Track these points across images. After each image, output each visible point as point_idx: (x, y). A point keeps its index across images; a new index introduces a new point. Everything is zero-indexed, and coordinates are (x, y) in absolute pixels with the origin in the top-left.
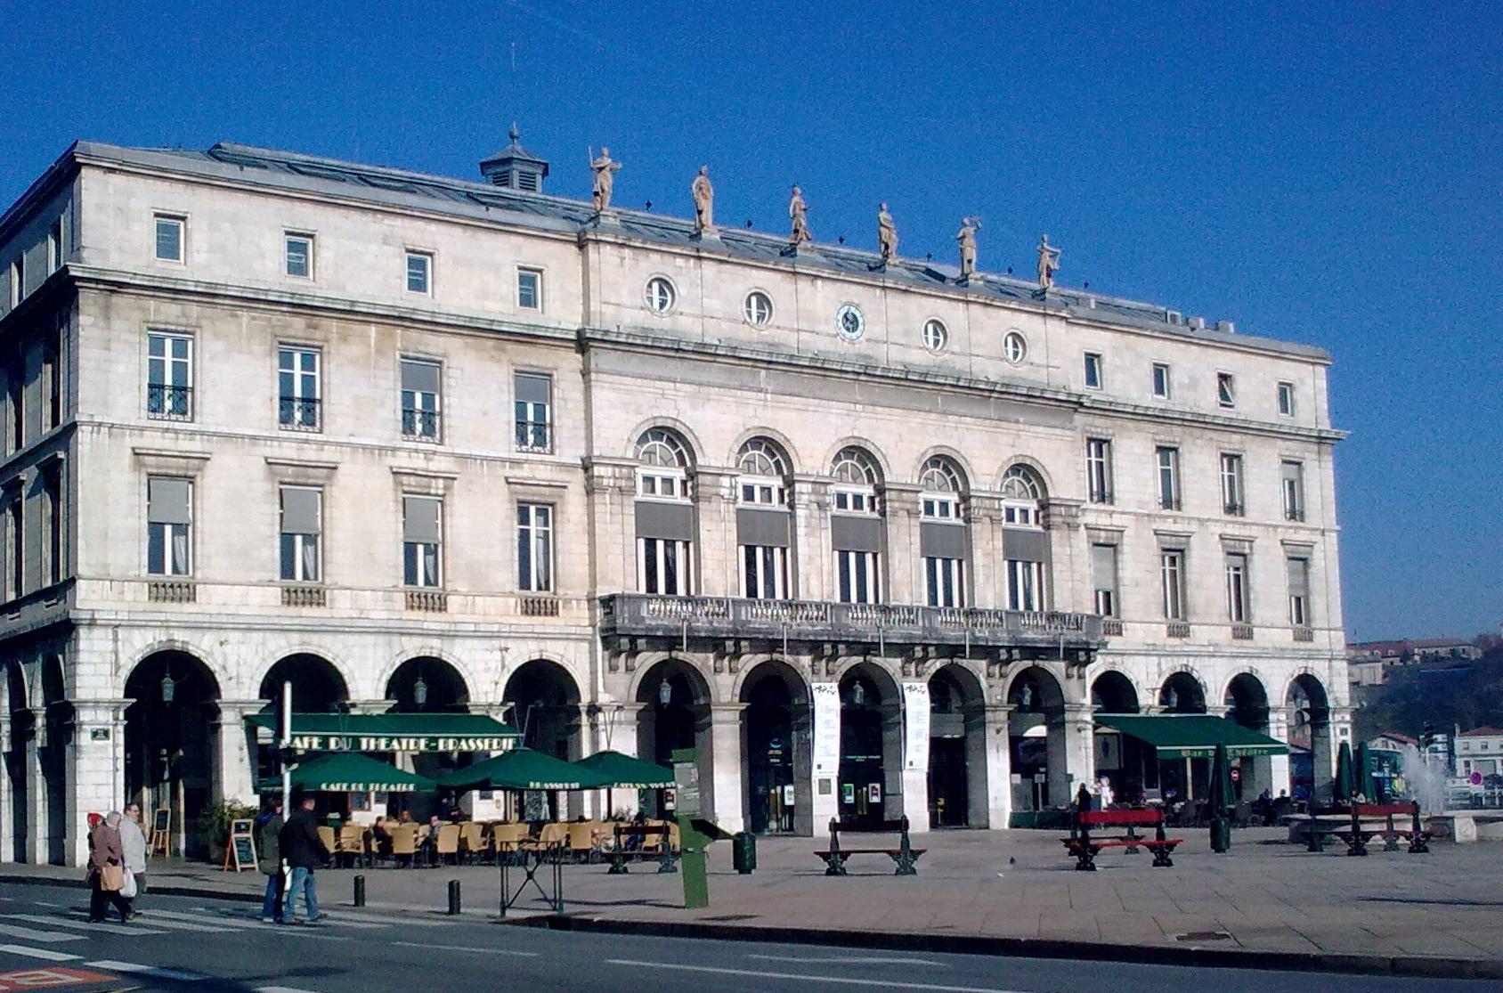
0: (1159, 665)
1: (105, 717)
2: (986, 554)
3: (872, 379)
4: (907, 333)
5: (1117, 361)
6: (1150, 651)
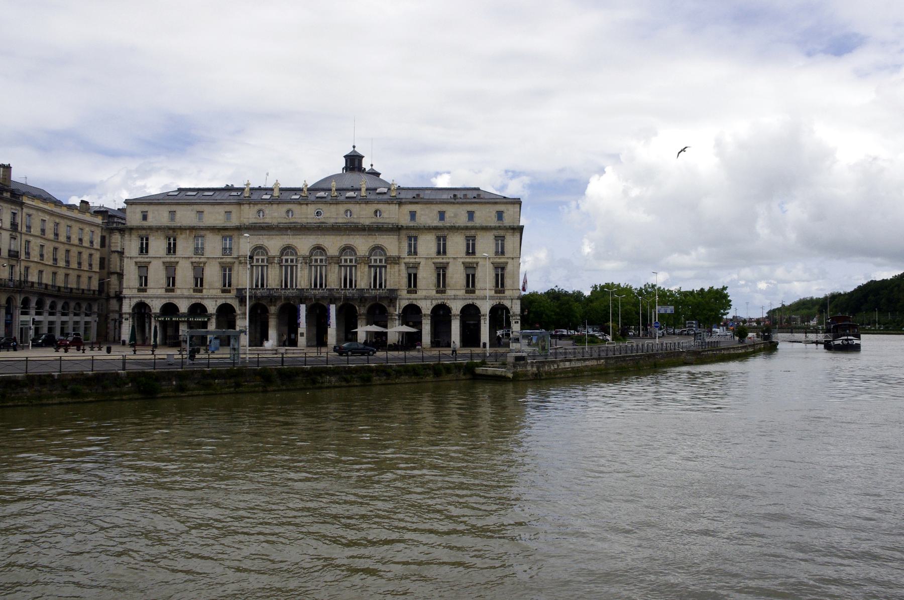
1: (128, 316)
6: (426, 298)
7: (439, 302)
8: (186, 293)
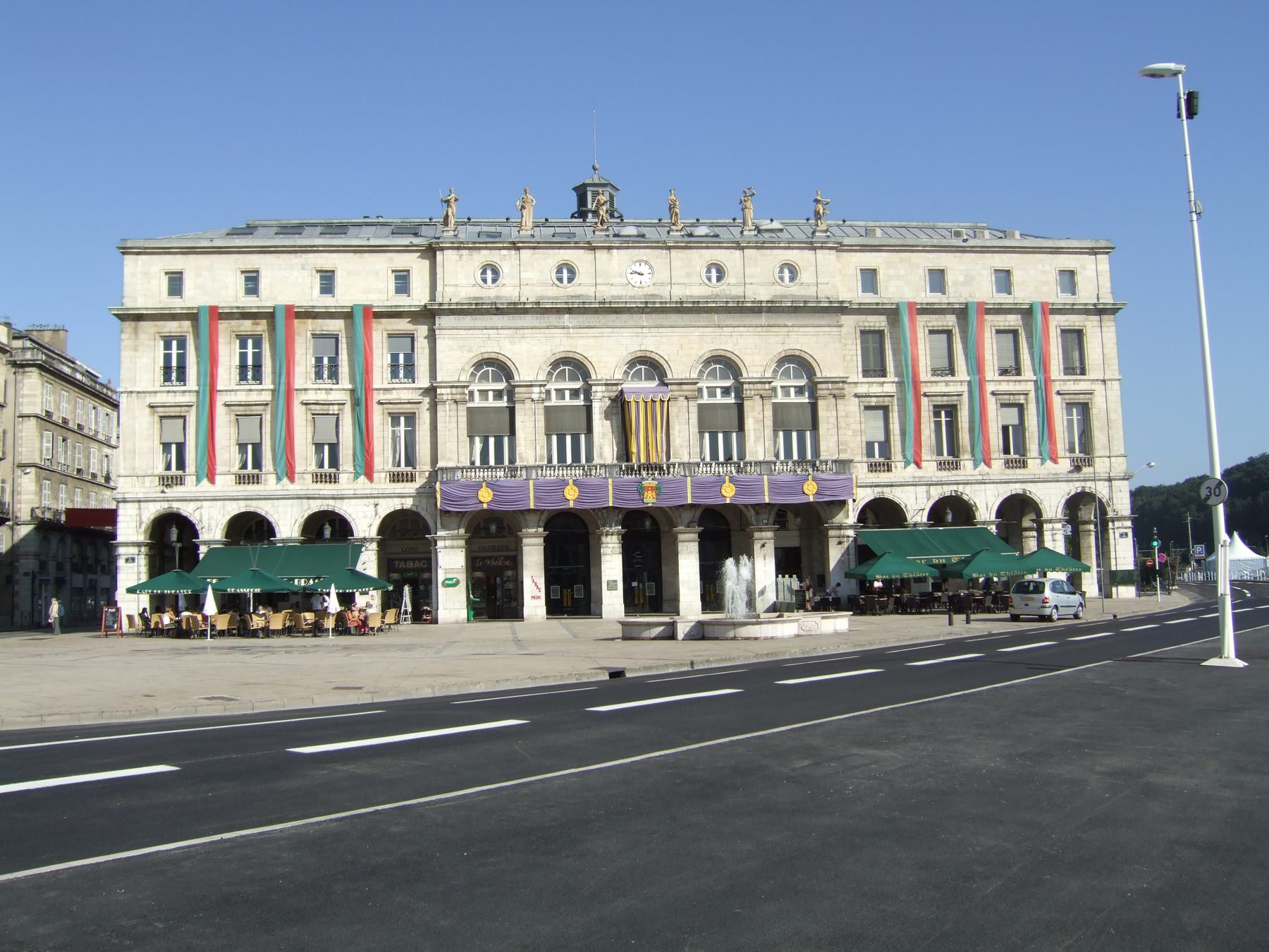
0: (928, 492)
2: (756, 421)
3: (649, 308)
4: (689, 275)
5: (891, 272)
7: (947, 491)
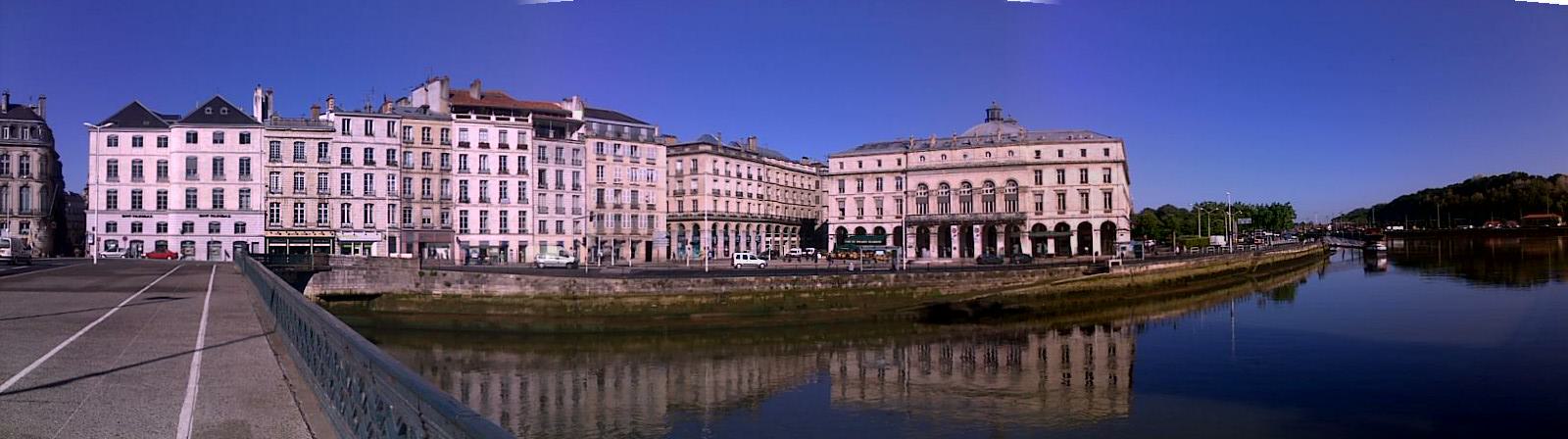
7: (1061, 221)
8: (871, 220)
